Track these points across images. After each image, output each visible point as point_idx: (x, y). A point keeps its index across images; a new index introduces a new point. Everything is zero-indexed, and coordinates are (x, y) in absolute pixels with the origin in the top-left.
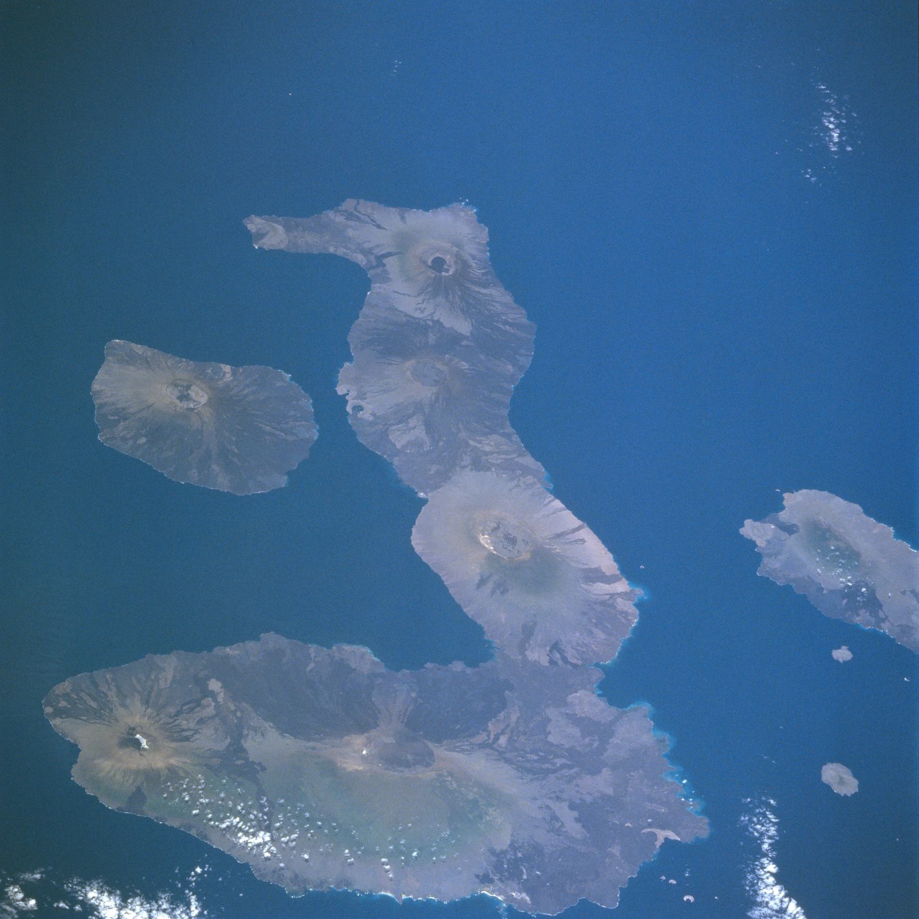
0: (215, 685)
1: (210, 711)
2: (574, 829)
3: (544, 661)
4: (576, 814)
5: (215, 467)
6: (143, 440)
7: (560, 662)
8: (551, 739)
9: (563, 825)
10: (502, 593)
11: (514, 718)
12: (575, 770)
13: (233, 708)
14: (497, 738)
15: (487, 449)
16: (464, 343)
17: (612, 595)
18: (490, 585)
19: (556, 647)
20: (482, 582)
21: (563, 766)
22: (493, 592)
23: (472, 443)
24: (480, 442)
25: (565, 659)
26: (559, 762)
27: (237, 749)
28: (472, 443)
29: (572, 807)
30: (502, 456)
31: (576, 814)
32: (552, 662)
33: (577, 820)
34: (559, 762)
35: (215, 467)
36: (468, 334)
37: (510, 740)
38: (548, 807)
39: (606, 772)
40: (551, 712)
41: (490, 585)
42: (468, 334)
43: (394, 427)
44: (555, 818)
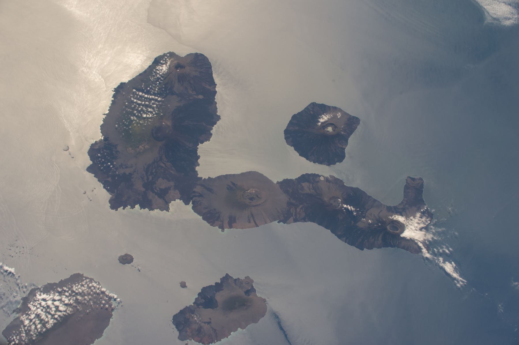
0: (201, 97)
1: (191, 92)
2: (121, 171)
3: (194, 190)
4: (127, 173)
5: (297, 128)
6: (312, 112)
7: (194, 194)
8: (160, 179)
9: (123, 168)
10: (227, 188)
11: (172, 172)
12: (146, 181)
13: (191, 98)
14: (163, 163)
15: (298, 210)
16: (353, 222)
17: (223, 222)
18: (232, 186)
19: (201, 196)
20: (234, 184)
21: (148, 179)
22: (228, 185)
23: (301, 206)
24: (301, 208)
25: (195, 196)
26: (151, 178)
27: (173, 93)
28: (301, 206)
29: (130, 174)
30: (294, 213)
31: (127, 173)
32: (195, 192)
33: (124, 173)
34: (151, 178)
35: (297, 128)
36: (357, 225)
37: (162, 167)
38: (132, 167)
39: (143, 189)
40: (172, 183)
41: (232, 186)
42: (357, 225)
43: (311, 185)
44: (127, 167)
